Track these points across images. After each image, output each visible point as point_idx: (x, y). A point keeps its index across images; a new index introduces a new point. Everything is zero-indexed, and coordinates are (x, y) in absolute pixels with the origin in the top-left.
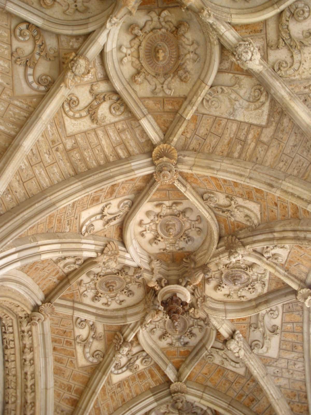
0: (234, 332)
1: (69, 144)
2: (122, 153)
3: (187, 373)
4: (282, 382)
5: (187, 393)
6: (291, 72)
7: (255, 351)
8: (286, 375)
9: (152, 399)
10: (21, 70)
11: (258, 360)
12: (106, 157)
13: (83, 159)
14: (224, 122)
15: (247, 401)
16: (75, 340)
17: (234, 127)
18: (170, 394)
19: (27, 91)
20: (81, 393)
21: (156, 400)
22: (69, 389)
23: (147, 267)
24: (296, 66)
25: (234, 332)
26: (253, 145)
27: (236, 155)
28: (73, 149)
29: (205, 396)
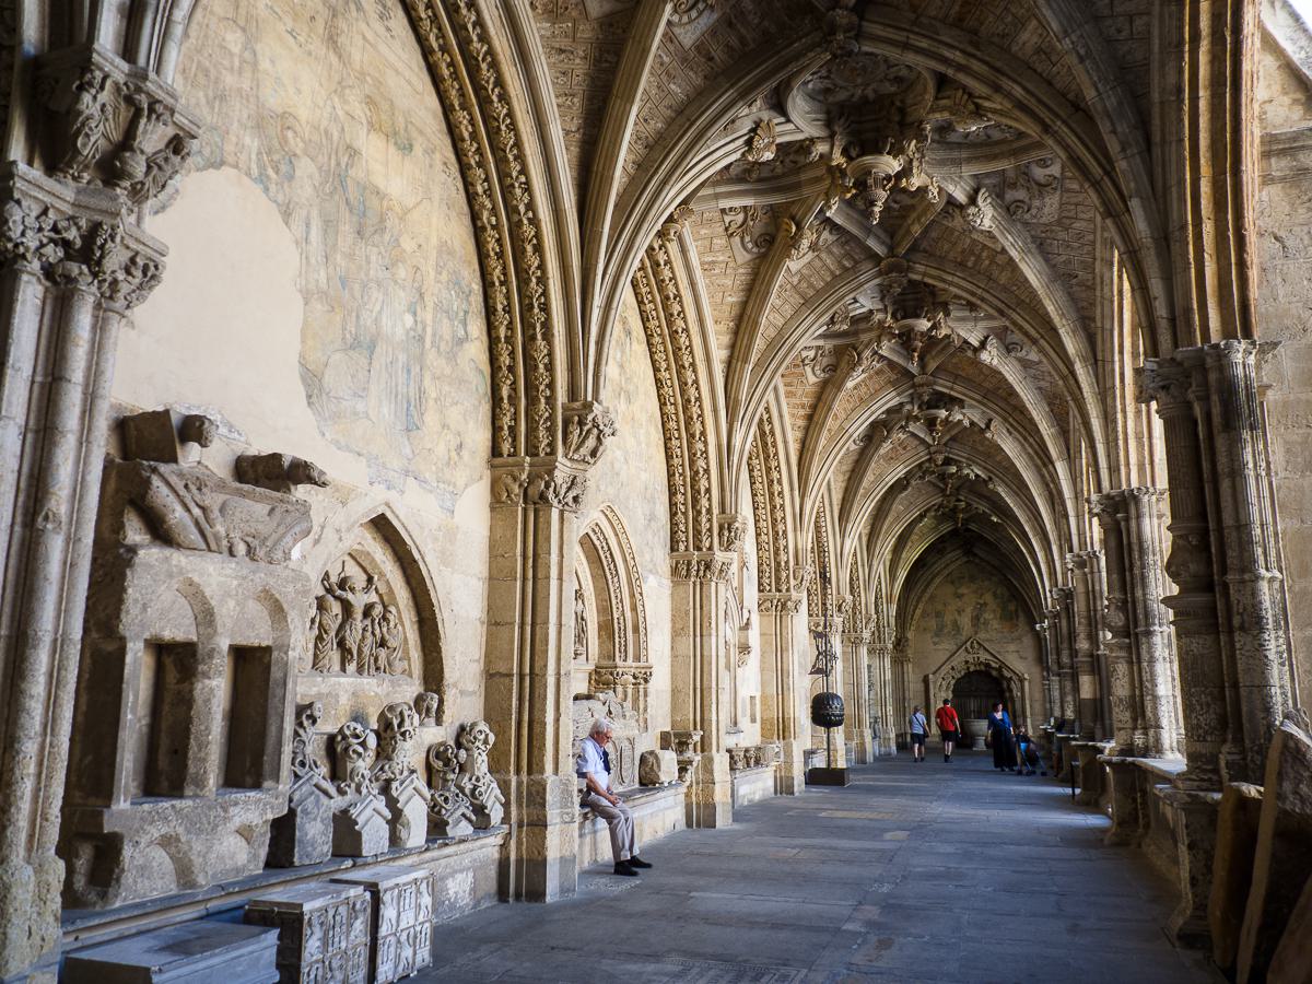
0: (986, 338)
1: (795, 280)
2: (847, 264)
3: (932, 366)
4: (1042, 384)
5: (935, 383)
6: (1027, 216)
7: (1013, 354)
8: (1048, 378)
9: (894, 394)
10: (737, 239)
11: (1018, 367)
12: (832, 273)
13: (811, 285)
14: (956, 233)
15: (1004, 394)
16: (803, 361)
17: (968, 241)
18: (913, 386)
19: (748, 257)
20: (814, 407)
21: (898, 395)
22: (803, 407)
23: (880, 307)
24: (1034, 211)
25: (986, 338)
26: (987, 262)
27: (970, 264)
28: (800, 281)
29: (956, 387)
